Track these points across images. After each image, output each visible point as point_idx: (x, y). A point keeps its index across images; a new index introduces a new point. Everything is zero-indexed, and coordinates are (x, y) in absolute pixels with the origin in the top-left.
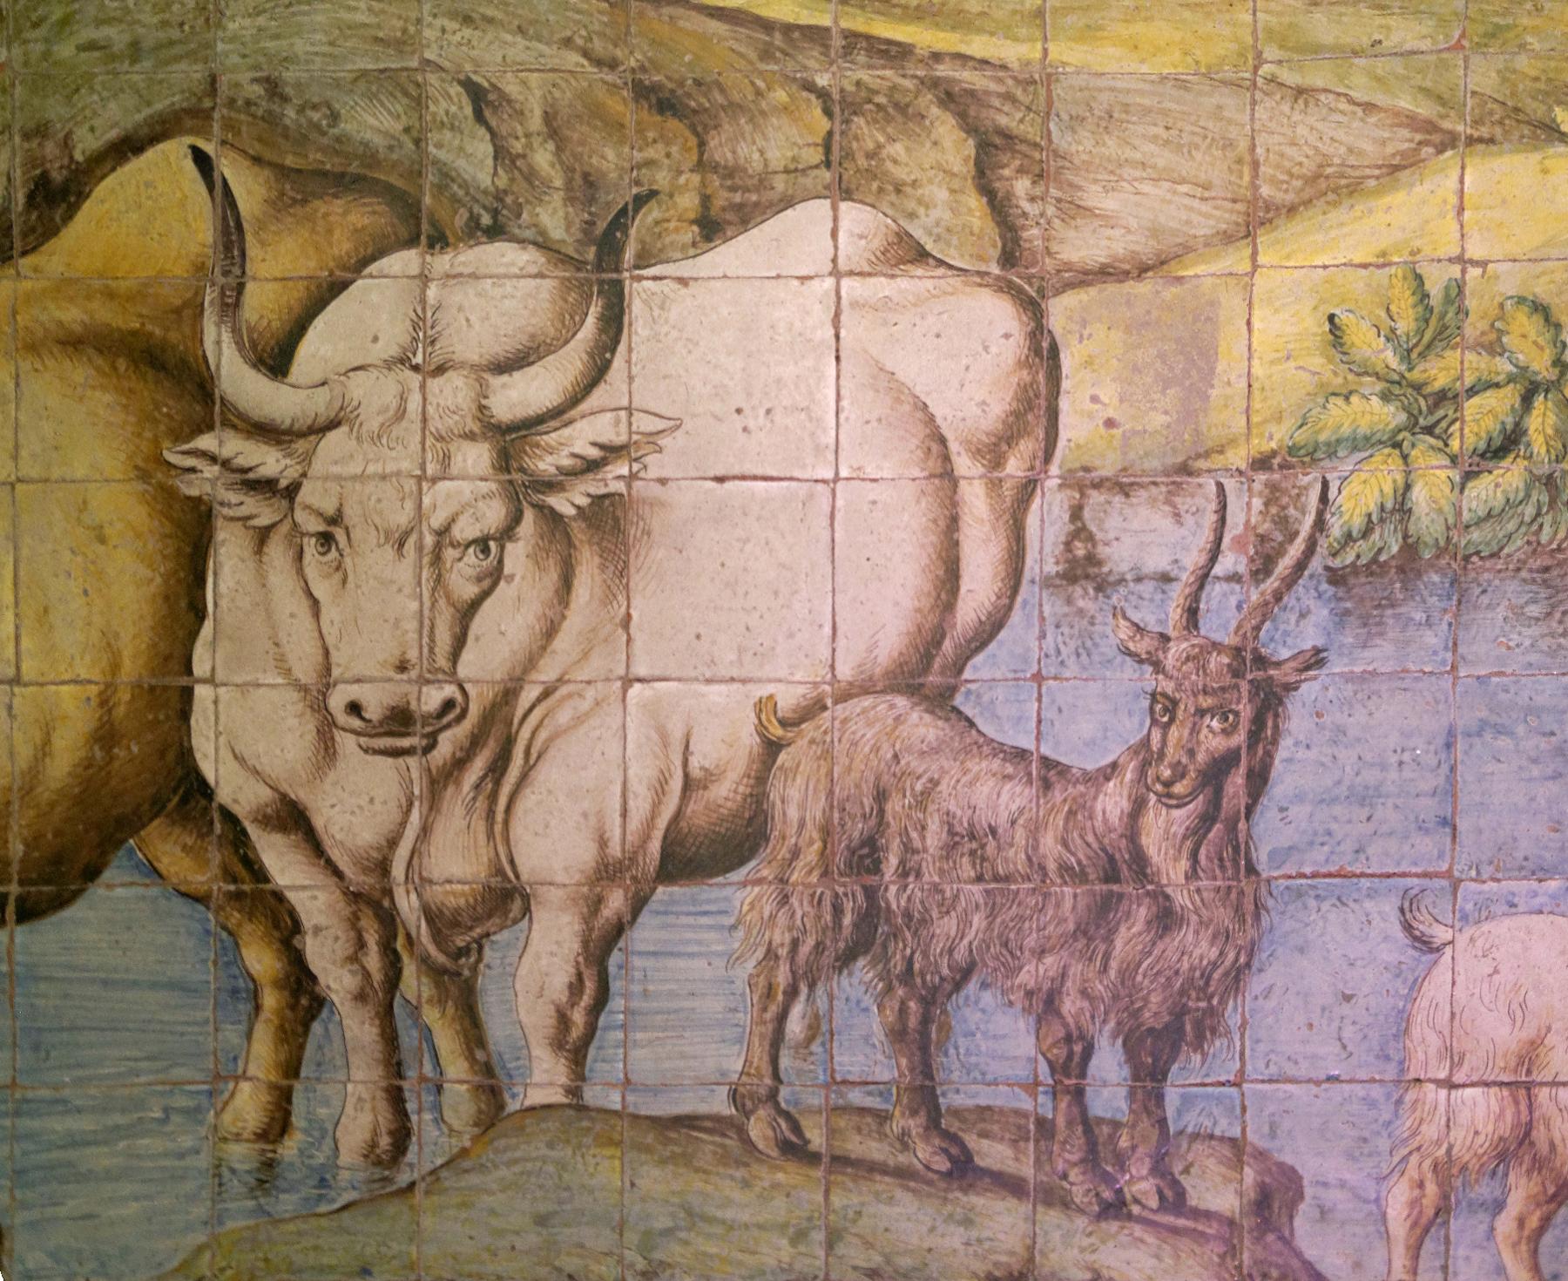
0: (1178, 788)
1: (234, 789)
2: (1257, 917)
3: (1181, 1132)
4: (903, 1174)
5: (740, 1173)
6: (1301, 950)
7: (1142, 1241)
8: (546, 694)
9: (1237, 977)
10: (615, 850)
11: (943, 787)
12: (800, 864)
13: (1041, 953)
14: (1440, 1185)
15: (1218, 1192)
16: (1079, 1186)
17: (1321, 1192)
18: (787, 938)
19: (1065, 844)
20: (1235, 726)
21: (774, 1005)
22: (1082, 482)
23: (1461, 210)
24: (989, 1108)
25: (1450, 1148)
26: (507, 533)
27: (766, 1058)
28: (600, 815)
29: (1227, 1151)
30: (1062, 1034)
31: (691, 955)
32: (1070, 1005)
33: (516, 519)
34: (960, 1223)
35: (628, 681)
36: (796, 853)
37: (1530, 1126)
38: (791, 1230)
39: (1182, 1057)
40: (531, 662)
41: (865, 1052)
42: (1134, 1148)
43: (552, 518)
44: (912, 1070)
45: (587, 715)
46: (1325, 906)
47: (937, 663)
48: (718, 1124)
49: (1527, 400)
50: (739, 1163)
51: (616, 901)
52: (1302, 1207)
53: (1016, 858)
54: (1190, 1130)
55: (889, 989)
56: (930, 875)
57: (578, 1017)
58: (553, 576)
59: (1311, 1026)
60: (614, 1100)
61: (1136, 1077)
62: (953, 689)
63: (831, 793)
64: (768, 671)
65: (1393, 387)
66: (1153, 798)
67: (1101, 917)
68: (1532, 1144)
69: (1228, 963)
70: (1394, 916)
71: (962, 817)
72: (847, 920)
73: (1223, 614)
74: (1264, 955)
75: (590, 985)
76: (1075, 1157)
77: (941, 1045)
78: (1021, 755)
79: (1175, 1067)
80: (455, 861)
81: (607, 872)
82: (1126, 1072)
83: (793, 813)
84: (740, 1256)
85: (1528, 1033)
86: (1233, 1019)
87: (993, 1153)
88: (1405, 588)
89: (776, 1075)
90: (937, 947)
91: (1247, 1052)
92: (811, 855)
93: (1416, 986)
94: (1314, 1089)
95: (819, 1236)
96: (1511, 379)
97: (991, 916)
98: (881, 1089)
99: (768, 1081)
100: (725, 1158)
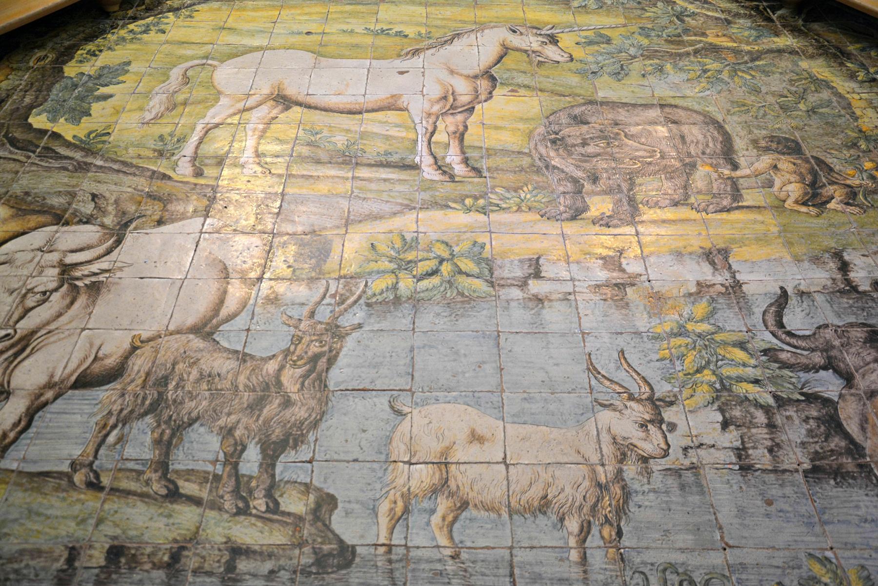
0: (299, 363)
2: (327, 404)
3: (281, 480)
4: (143, 496)
5: (61, 495)
6: (345, 414)
7: (254, 525)
8: (49, 332)
9: (315, 425)
10: (56, 379)
11: (202, 361)
12: (133, 384)
13: (229, 414)
14: (405, 502)
15: (294, 503)
16: (229, 504)
17: (347, 505)
18: (119, 408)
19: (248, 379)
20: (324, 345)
21: (104, 429)
23: (417, 222)
24: (193, 470)
25: (409, 489)
26: (56, 290)
27: (94, 450)
28: (54, 368)
29: (302, 488)
30: (233, 442)
31: (74, 413)
32: (237, 433)
33: (61, 286)
34: (165, 516)
35: (83, 329)
36: (132, 381)
37: (447, 480)
38: (79, 518)
39: (287, 452)
40: (48, 323)
41: (140, 442)
42: (258, 486)
43: (76, 286)
44: (160, 455)
45: (63, 339)
46: (356, 400)
47: (209, 326)
48: (60, 475)
49: (441, 263)
50: (64, 490)
51: (49, 394)
52: (336, 511)
53: (226, 384)
54: (286, 479)
55: (159, 425)
56: (188, 387)
57: (12, 435)
58: (68, 300)
59: (347, 441)
60: (14, 466)
61: (264, 459)
62: (213, 333)
63: (154, 362)
64: (142, 327)
66: (288, 365)
68: (448, 486)
69: (312, 419)
70: (386, 404)
71: (207, 369)
72: (147, 402)
73: (324, 314)
74: (328, 417)
75: (23, 424)
76: (230, 489)
77: (176, 446)
78: (237, 352)
79: (282, 456)
81: (50, 385)
82: (260, 457)
83: (136, 368)
84: (47, 530)
85: (446, 443)
86: (311, 437)
87: (188, 488)
88: (395, 308)
89: (95, 457)
90: (184, 412)
91: (317, 450)
92: (139, 381)
93: (395, 427)
94: (347, 464)
95: (92, 521)
96: (435, 258)
97: (211, 402)
98: (143, 462)
99: (91, 458)
100: (57, 489)
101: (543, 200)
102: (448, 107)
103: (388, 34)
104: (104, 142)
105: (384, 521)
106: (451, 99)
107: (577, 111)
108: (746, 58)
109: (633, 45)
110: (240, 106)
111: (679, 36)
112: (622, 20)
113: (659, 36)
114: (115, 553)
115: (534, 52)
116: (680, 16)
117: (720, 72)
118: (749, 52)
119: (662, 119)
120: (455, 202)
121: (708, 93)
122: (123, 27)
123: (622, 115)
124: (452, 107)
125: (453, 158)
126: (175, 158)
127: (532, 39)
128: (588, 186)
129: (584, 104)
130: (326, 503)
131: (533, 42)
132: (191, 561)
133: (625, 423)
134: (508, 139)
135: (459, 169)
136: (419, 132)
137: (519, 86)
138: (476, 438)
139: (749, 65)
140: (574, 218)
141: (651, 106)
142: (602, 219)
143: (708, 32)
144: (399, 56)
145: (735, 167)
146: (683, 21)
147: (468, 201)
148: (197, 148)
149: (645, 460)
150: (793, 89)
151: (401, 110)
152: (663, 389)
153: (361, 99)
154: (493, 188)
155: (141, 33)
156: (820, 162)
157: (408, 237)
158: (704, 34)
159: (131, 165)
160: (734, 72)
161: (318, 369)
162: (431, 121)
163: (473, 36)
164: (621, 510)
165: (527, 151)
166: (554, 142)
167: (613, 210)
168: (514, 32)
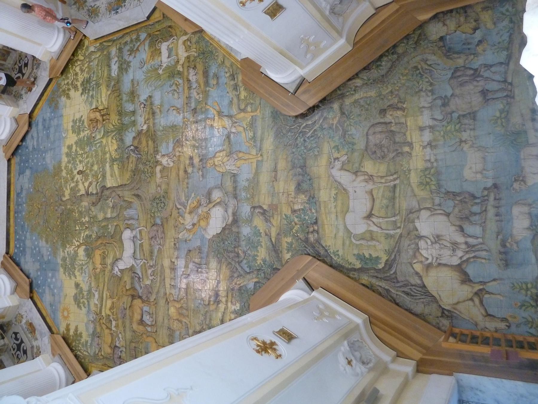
1: (459, 262)
15: (486, 193)
16: (486, 202)
22: (433, 205)
65: (426, 186)
67: (465, 202)
80: (463, 246)
81: (464, 236)
87: (484, 209)
104: (389, 250)
105: (488, 180)
114: (497, 215)
124: (371, 179)
130: (485, 189)
132: (497, 205)
133: (466, 147)
135: (395, 176)
138: (471, 168)
145: (391, 123)
149: (473, 144)
152: (458, 140)
157: (419, 184)
159: (397, 242)
161: (455, 194)
164: (484, 147)
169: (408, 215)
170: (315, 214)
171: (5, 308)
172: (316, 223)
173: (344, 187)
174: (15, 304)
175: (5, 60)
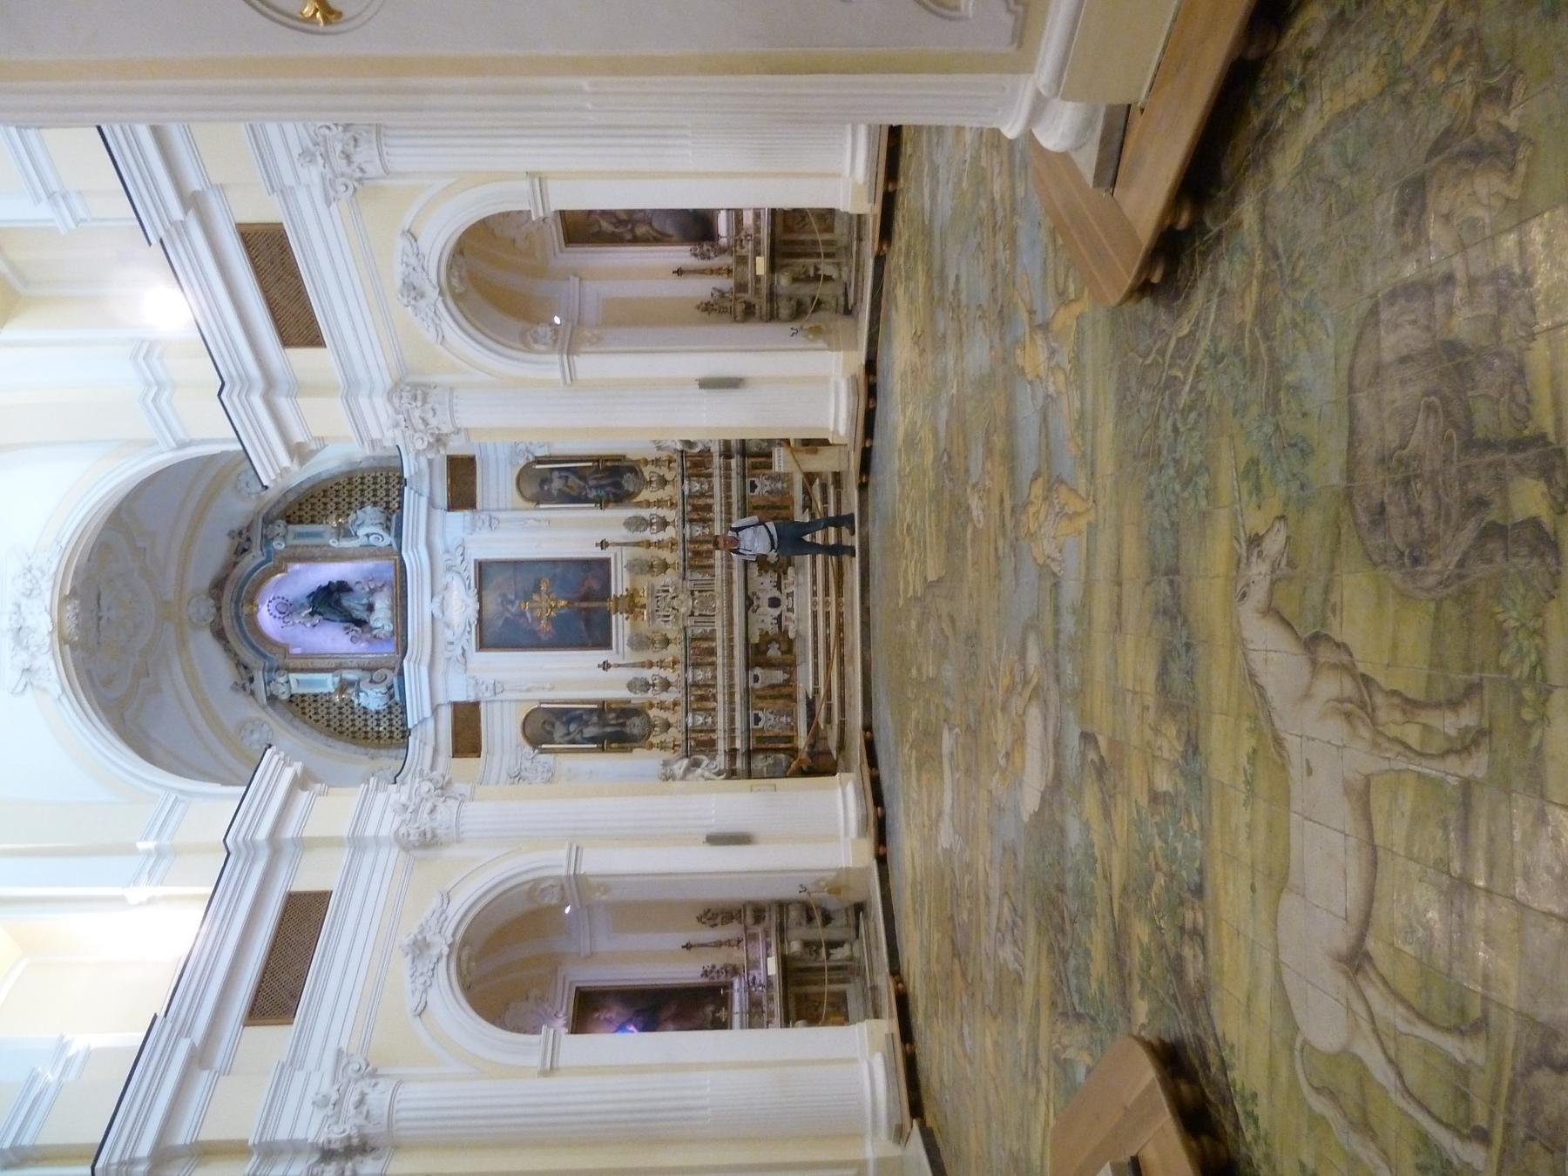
101: (1522, 591)
102: (1363, 714)
103: (1252, 776)
106: (1349, 706)
107: (1364, 519)
108: (1274, 267)
109: (1260, 428)
110: (1366, 1027)
111: (1244, 361)
112: (1225, 440)
113: (1245, 390)
115: (1273, 571)
116: (1217, 359)
117: (1295, 304)
118: (1266, 262)
119: (1373, 391)
120: (1528, 736)
121: (1328, 322)
122: (1248, 1146)
123: (1369, 450)
125: (1450, 723)
126: (1455, 1162)
127: (1254, 571)
128: (1494, 515)
129: (1352, 508)
131: (1259, 571)
134: (1414, 632)
135: (1468, 717)
136: (1404, 766)
137: (1326, 600)
139: (1284, 261)
140: (1555, 546)
141: (1351, 405)
142: (1554, 498)
143: (1237, 321)
144: (1283, 768)
146: (1223, 356)
147: (1528, 715)
148: (1439, 1121)
150: (1318, 196)
151: (1368, 785)
153: (1353, 841)
154: (1500, 669)
155: (1257, 1127)
156: (1437, 148)
158: (1241, 326)
160: (1295, 283)
162: (1386, 745)
163: (1252, 655)
165: (1432, 606)
166: (1416, 561)
167: (1537, 478)
168: (1244, 595)
169: (1528, 1072)
170: (1198, 843)
171: (839, 871)
172: (1199, 891)
173: (1278, 724)
174: (860, 865)
175: (830, 229)
